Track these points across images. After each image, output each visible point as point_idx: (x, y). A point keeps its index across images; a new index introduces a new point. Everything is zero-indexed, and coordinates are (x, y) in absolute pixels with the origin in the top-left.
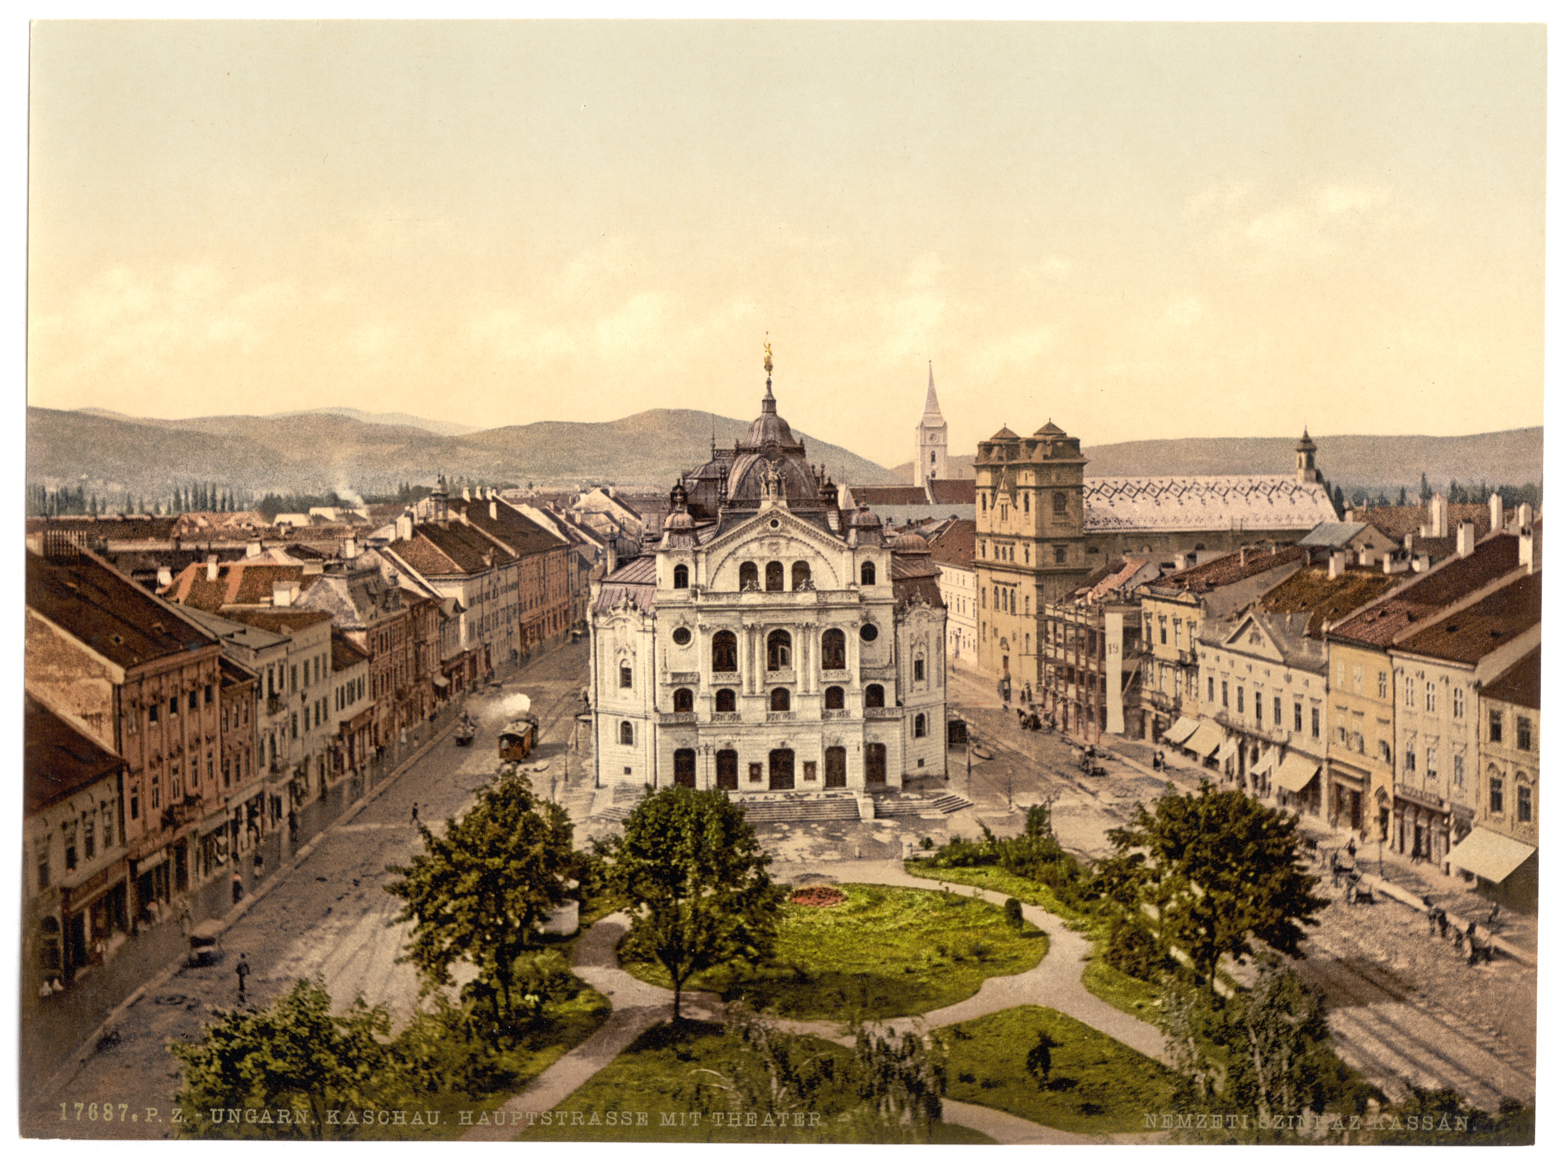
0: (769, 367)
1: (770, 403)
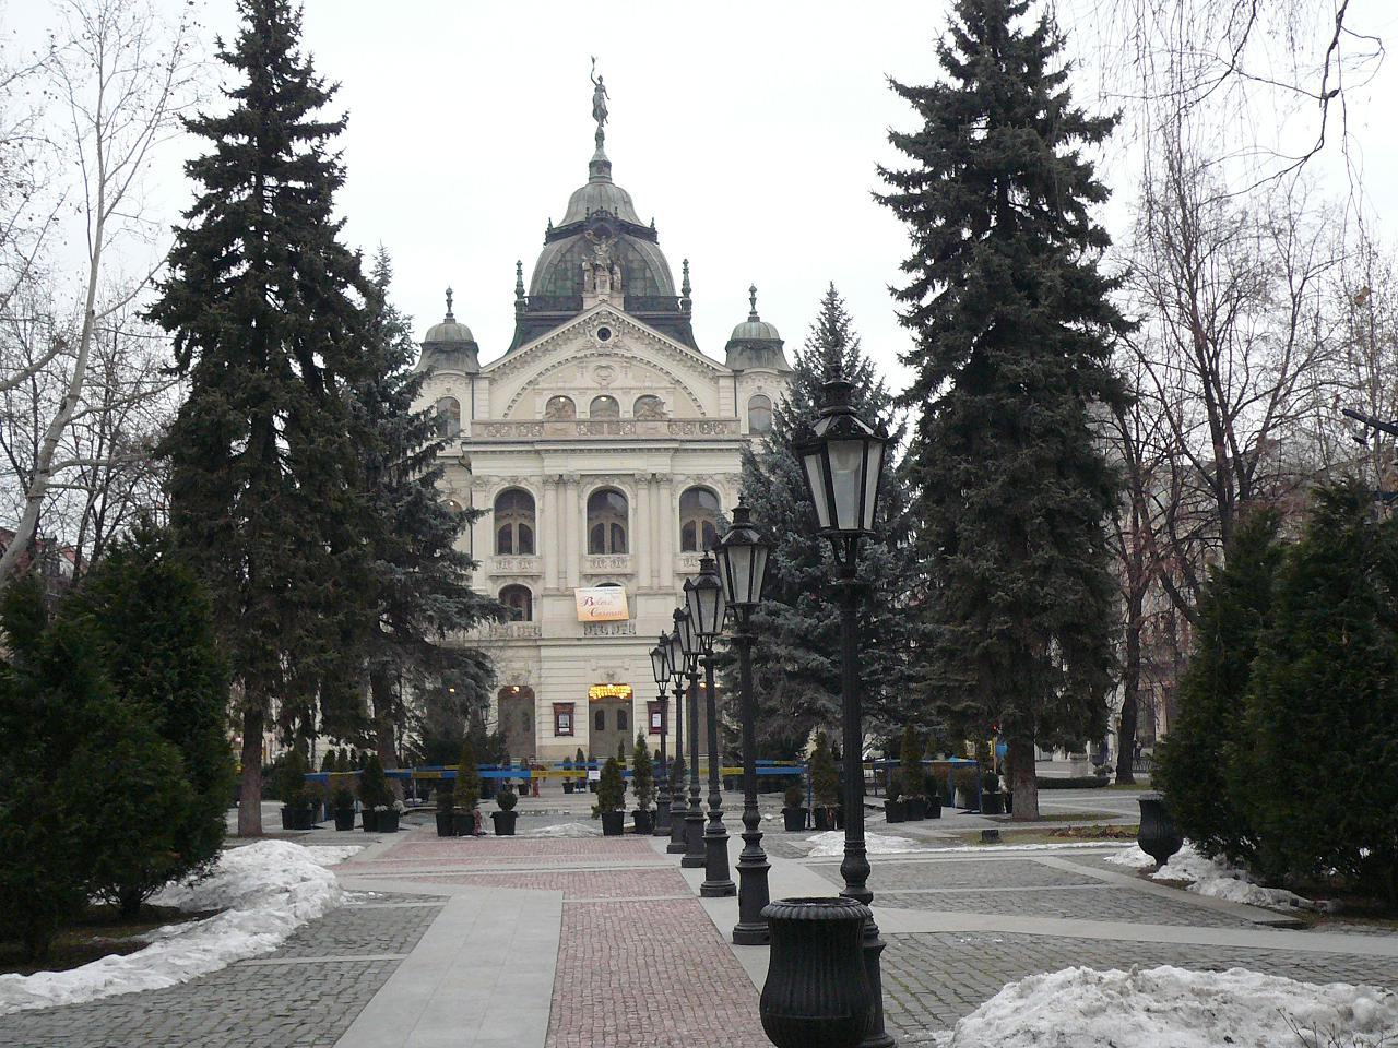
0: (600, 113)
1: (600, 167)
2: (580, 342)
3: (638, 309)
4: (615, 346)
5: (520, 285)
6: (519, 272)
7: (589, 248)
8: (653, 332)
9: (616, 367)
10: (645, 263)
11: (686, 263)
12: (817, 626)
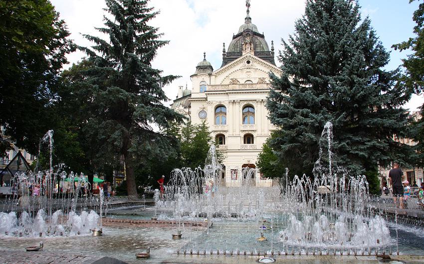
0: (248, 5)
1: (248, 19)
4: (252, 66)
6: (224, 46)
10: (261, 43)
11: (272, 42)
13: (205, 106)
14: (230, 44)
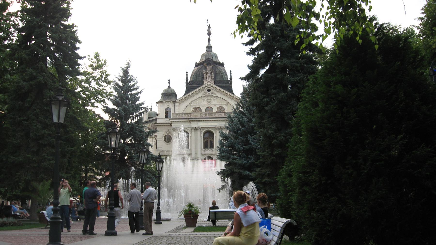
0: (209, 34)
1: (209, 48)
2: (203, 92)
3: (218, 84)
4: (212, 93)
5: (187, 78)
6: (187, 75)
7: (206, 69)
8: (222, 90)
9: (212, 99)
10: (220, 72)
11: (231, 71)
12: (247, 163)
13: (170, 131)
14: (193, 72)
